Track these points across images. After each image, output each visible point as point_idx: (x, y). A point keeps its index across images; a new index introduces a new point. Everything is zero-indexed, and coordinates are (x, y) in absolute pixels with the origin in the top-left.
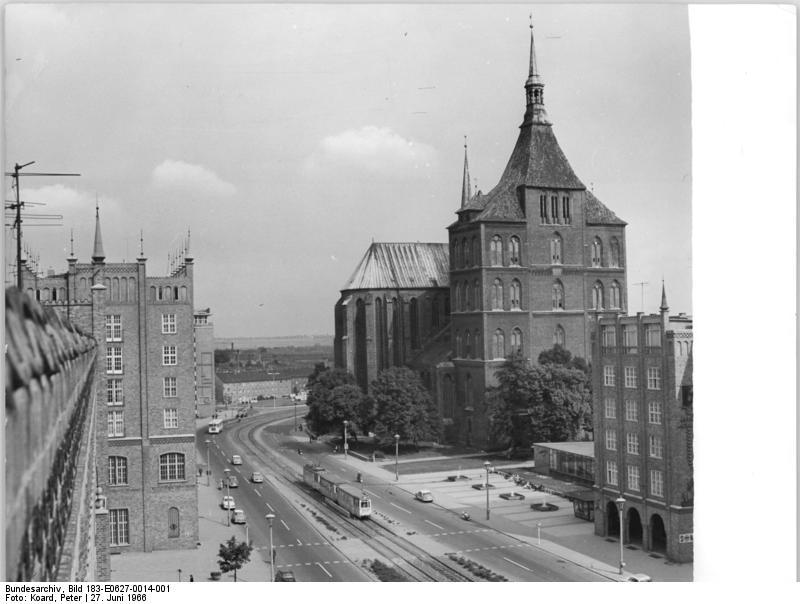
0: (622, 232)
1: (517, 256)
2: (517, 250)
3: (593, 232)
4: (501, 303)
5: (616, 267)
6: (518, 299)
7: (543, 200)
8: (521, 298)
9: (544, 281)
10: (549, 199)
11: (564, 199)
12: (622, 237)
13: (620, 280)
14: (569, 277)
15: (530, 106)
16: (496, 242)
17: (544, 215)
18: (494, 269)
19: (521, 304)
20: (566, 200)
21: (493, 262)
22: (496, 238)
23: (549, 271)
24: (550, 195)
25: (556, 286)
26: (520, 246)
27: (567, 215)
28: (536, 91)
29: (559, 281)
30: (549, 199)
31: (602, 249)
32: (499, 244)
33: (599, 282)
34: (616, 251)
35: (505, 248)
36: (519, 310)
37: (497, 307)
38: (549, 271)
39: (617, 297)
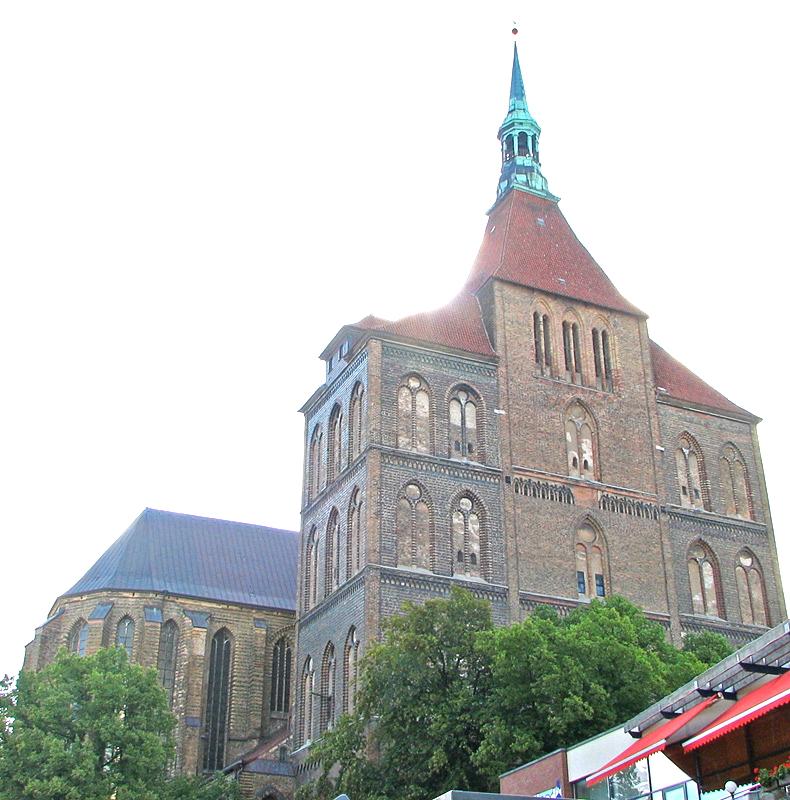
0: (752, 434)
1: (472, 439)
2: (471, 424)
3: (672, 417)
4: (423, 551)
5: (744, 517)
6: (476, 548)
7: (540, 323)
8: (483, 547)
9: (548, 512)
10: (556, 325)
11: (595, 332)
12: (754, 448)
13: (758, 552)
14: (623, 519)
15: (509, 170)
16: (413, 392)
17: (542, 357)
18: (405, 457)
19: (485, 563)
20: (600, 339)
21: (403, 440)
22: (414, 384)
23: (565, 493)
24: (557, 314)
25: (585, 535)
26: (479, 415)
27: (605, 373)
28: (523, 136)
29: (589, 523)
30: (556, 325)
31: (702, 467)
32: (423, 400)
33: (701, 544)
34: (741, 482)
35: (439, 412)
36: (478, 579)
37: (415, 561)
38: (565, 493)
39: (757, 595)
